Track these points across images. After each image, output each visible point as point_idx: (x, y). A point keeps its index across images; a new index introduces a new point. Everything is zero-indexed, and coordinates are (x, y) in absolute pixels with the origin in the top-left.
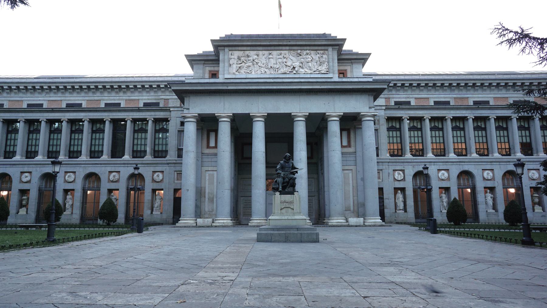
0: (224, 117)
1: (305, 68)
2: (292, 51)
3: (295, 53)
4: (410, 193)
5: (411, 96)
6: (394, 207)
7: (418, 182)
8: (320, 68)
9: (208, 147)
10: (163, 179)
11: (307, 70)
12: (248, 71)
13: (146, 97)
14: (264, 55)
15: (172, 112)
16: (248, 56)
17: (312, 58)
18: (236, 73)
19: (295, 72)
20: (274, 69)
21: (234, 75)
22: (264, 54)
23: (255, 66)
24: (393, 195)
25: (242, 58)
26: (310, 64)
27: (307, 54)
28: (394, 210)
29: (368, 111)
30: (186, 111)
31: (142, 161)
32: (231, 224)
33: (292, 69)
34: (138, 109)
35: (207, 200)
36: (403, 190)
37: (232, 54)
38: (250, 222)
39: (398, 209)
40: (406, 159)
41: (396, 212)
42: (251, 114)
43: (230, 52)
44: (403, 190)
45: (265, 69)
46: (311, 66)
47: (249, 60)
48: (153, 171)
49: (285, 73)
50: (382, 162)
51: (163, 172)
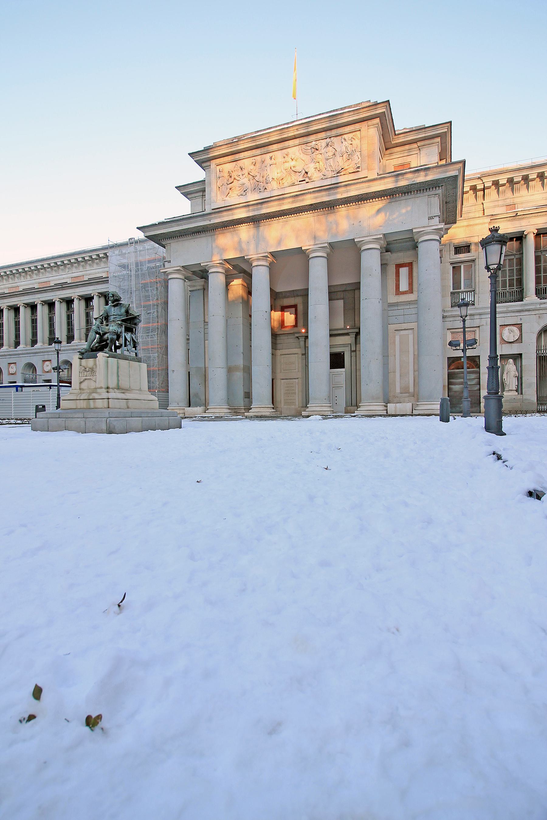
19: (307, 180)
39: (506, 389)
40: (526, 305)
43: (218, 168)
50: (480, 314)
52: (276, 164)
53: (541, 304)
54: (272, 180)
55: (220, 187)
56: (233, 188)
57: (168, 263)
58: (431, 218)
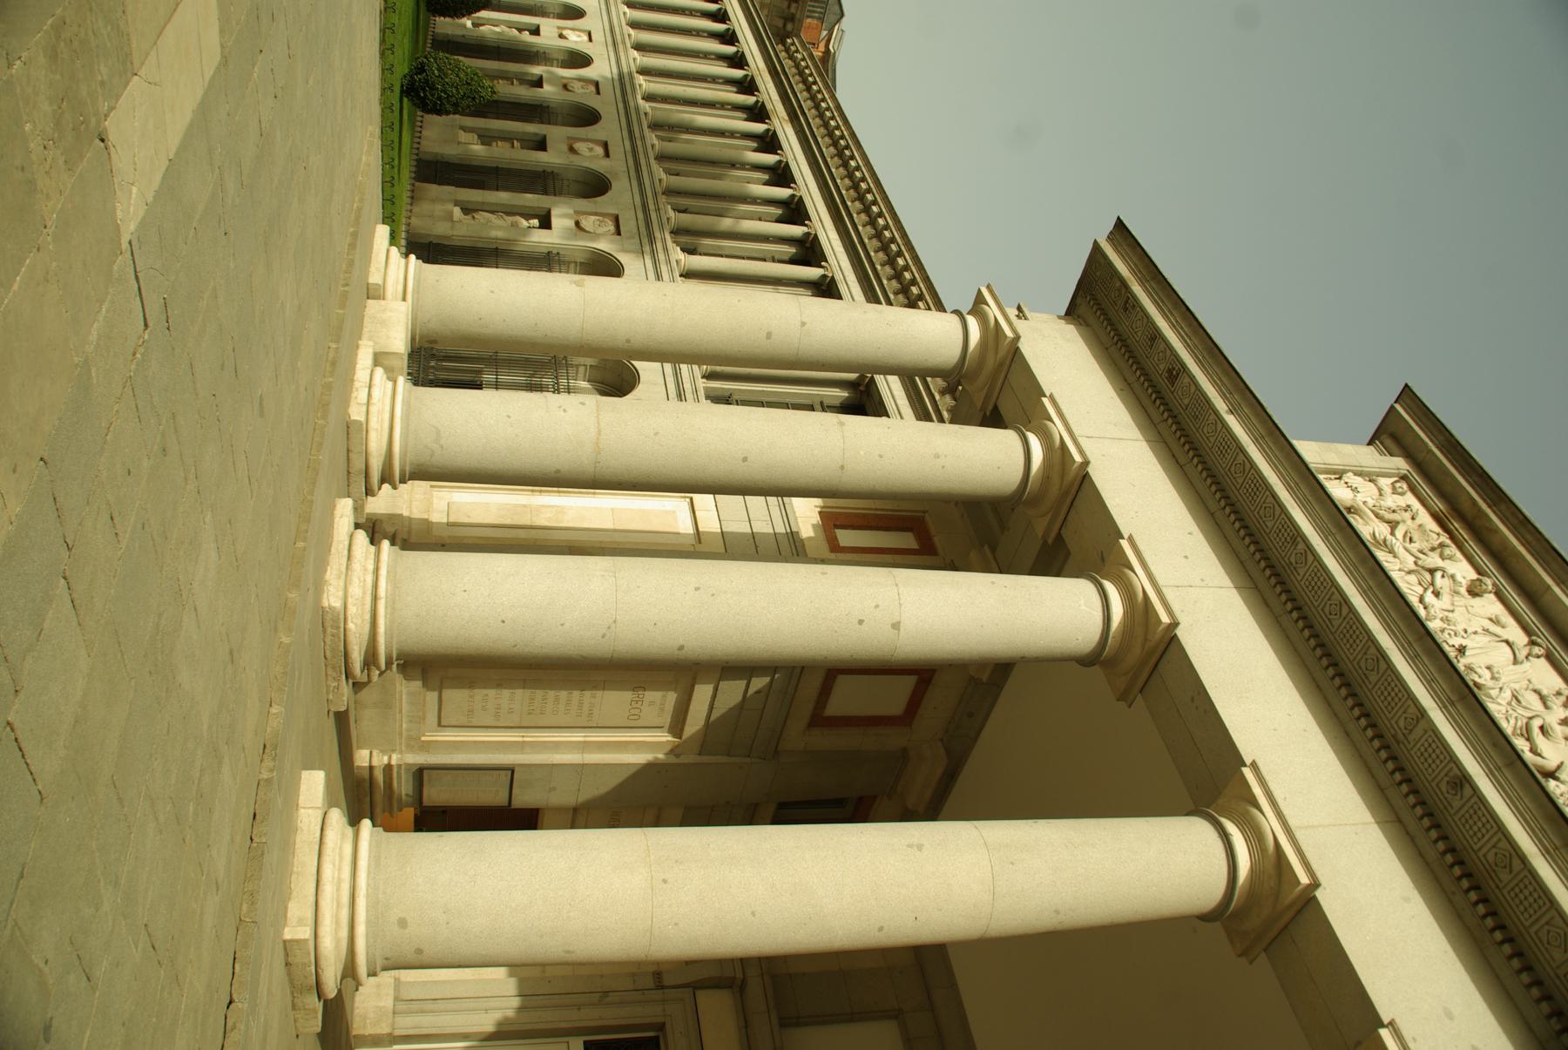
0: (1046, 437)
14: (1495, 621)
54: (1457, 646)
56: (1357, 517)
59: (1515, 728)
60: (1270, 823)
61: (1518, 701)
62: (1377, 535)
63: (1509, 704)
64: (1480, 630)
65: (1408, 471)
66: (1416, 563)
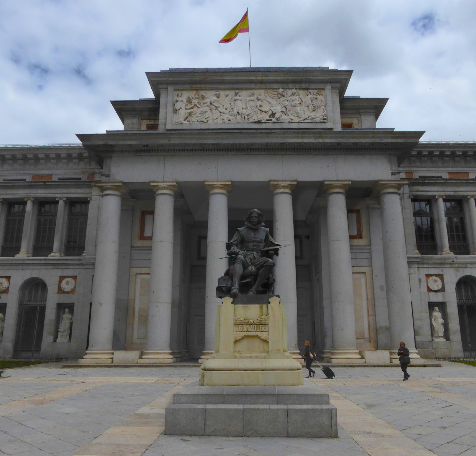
0: (164, 188)
1: (290, 115)
2: (269, 91)
3: (274, 93)
4: (453, 310)
5: (442, 169)
6: (430, 333)
7: (464, 294)
8: (313, 115)
9: (142, 237)
10: (75, 287)
11: (293, 118)
12: (203, 120)
13: (63, 171)
14: (227, 96)
15: (93, 188)
16: (203, 98)
17: (300, 100)
18: (185, 122)
19: (274, 120)
20: (243, 116)
21: (181, 125)
22: (227, 94)
23: (214, 111)
24: (428, 314)
25: (194, 101)
26: (298, 108)
27: (293, 94)
28: (431, 337)
29: (389, 179)
30: (104, 179)
31: (46, 260)
32: (171, 361)
33: (270, 117)
34: (43, 184)
35: (136, 319)
36: (442, 306)
37: (179, 95)
38: (202, 357)
39: (436, 335)
40: (445, 258)
41: (433, 340)
42: (206, 183)
43: (176, 93)
44: (442, 306)
45: (228, 116)
46: (299, 111)
47: (204, 103)
48: (60, 277)
49: (259, 122)
51: (76, 276)
52: (241, 100)
53: (456, 258)
54: (237, 113)
55: (178, 110)
56: (192, 114)
57: (106, 177)
58: (393, 174)
59: (260, 114)
60: (283, 184)
61: (252, 107)
62: (200, 113)
63: (252, 109)
64: (230, 102)
65: (173, 88)
66: (208, 107)
